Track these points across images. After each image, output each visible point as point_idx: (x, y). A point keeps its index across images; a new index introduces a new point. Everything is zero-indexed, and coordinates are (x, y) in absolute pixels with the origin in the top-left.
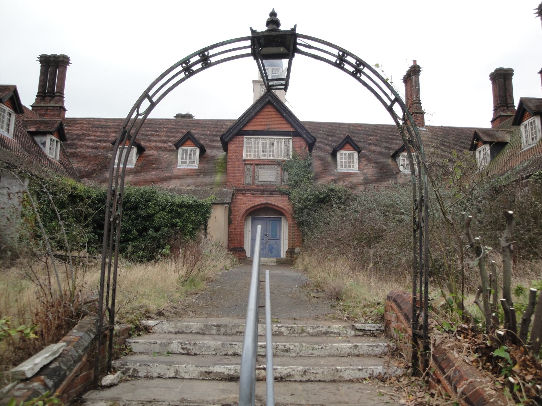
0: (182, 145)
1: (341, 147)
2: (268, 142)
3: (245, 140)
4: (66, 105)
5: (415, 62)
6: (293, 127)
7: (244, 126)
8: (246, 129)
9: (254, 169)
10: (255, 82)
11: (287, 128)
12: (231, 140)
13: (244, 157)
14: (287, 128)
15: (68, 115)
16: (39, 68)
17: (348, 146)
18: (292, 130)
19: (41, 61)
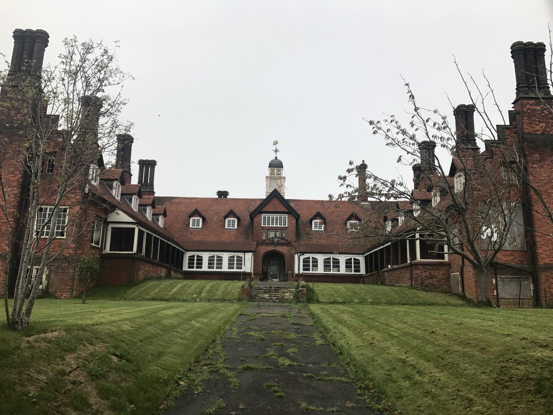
0: (228, 217)
1: (315, 218)
2: (275, 217)
3: (262, 216)
4: (155, 190)
5: (363, 161)
6: (287, 209)
7: (262, 209)
8: (263, 210)
9: (267, 232)
10: (266, 177)
11: (285, 210)
12: (255, 216)
13: (262, 225)
14: (285, 210)
15: (156, 195)
16: (138, 168)
17: (318, 217)
18: (287, 211)
19: (139, 164)
